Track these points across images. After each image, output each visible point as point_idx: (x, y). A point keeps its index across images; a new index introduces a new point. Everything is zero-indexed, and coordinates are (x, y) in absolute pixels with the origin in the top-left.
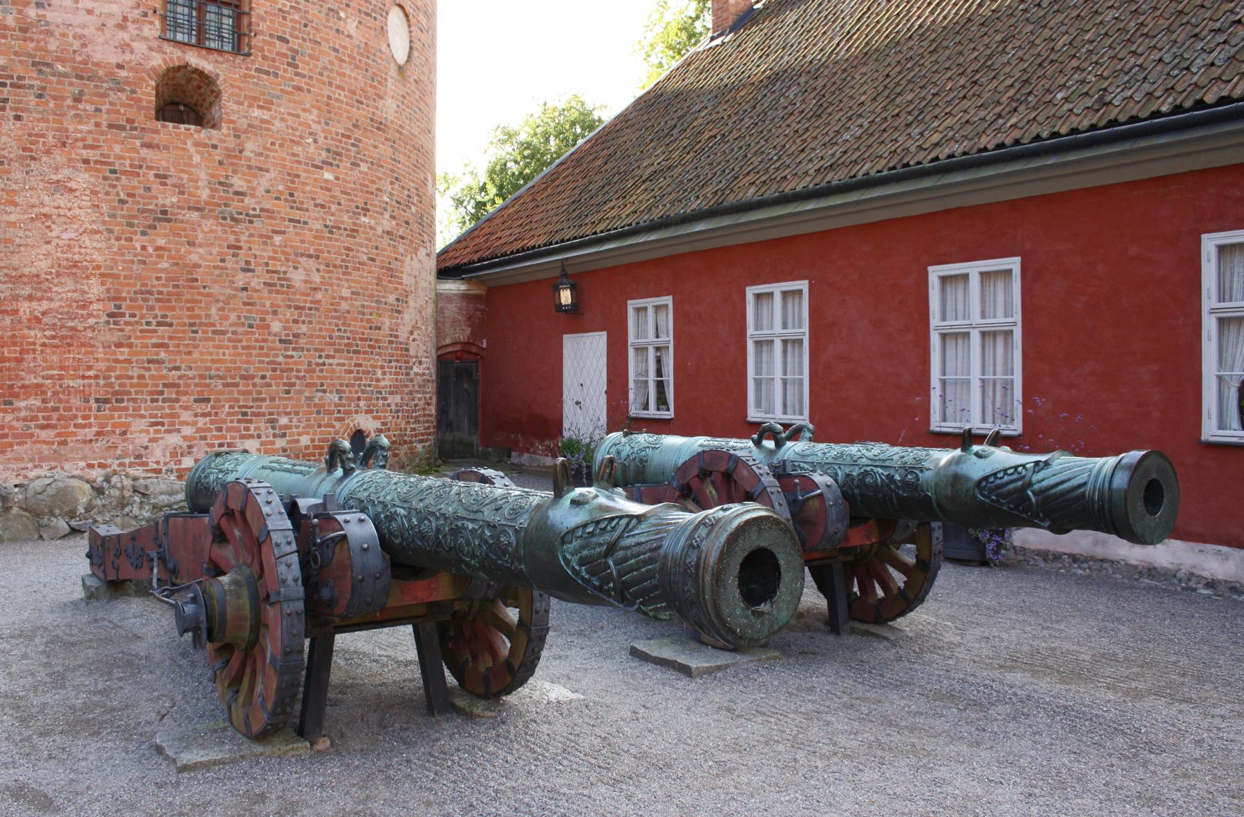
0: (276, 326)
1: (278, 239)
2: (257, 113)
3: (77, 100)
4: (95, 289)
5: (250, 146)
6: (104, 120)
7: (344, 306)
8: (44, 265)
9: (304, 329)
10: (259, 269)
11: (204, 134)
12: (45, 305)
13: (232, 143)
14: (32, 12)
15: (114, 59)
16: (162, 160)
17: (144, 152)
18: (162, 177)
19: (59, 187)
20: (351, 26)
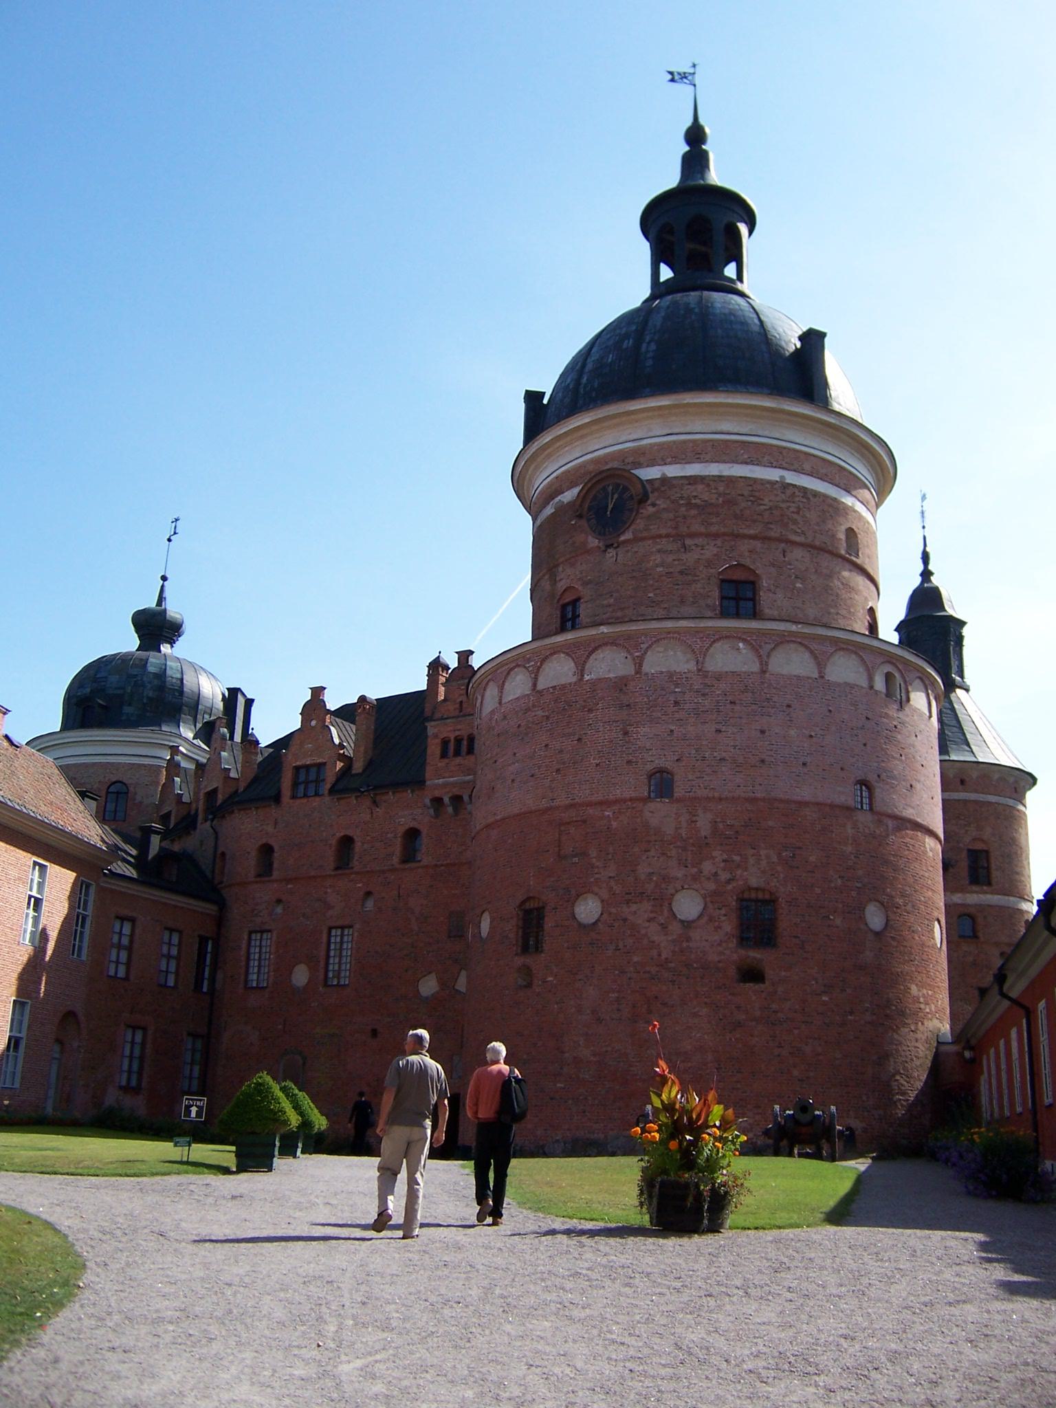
0: (796, 1073)
1: (796, 1032)
4: (710, 1057)
5: (780, 989)
9: (812, 1074)
11: (758, 987)
14: (685, 945)
15: (716, 959)
18: (738, 1008)
19: (695, 1015)
20: (838, 922)
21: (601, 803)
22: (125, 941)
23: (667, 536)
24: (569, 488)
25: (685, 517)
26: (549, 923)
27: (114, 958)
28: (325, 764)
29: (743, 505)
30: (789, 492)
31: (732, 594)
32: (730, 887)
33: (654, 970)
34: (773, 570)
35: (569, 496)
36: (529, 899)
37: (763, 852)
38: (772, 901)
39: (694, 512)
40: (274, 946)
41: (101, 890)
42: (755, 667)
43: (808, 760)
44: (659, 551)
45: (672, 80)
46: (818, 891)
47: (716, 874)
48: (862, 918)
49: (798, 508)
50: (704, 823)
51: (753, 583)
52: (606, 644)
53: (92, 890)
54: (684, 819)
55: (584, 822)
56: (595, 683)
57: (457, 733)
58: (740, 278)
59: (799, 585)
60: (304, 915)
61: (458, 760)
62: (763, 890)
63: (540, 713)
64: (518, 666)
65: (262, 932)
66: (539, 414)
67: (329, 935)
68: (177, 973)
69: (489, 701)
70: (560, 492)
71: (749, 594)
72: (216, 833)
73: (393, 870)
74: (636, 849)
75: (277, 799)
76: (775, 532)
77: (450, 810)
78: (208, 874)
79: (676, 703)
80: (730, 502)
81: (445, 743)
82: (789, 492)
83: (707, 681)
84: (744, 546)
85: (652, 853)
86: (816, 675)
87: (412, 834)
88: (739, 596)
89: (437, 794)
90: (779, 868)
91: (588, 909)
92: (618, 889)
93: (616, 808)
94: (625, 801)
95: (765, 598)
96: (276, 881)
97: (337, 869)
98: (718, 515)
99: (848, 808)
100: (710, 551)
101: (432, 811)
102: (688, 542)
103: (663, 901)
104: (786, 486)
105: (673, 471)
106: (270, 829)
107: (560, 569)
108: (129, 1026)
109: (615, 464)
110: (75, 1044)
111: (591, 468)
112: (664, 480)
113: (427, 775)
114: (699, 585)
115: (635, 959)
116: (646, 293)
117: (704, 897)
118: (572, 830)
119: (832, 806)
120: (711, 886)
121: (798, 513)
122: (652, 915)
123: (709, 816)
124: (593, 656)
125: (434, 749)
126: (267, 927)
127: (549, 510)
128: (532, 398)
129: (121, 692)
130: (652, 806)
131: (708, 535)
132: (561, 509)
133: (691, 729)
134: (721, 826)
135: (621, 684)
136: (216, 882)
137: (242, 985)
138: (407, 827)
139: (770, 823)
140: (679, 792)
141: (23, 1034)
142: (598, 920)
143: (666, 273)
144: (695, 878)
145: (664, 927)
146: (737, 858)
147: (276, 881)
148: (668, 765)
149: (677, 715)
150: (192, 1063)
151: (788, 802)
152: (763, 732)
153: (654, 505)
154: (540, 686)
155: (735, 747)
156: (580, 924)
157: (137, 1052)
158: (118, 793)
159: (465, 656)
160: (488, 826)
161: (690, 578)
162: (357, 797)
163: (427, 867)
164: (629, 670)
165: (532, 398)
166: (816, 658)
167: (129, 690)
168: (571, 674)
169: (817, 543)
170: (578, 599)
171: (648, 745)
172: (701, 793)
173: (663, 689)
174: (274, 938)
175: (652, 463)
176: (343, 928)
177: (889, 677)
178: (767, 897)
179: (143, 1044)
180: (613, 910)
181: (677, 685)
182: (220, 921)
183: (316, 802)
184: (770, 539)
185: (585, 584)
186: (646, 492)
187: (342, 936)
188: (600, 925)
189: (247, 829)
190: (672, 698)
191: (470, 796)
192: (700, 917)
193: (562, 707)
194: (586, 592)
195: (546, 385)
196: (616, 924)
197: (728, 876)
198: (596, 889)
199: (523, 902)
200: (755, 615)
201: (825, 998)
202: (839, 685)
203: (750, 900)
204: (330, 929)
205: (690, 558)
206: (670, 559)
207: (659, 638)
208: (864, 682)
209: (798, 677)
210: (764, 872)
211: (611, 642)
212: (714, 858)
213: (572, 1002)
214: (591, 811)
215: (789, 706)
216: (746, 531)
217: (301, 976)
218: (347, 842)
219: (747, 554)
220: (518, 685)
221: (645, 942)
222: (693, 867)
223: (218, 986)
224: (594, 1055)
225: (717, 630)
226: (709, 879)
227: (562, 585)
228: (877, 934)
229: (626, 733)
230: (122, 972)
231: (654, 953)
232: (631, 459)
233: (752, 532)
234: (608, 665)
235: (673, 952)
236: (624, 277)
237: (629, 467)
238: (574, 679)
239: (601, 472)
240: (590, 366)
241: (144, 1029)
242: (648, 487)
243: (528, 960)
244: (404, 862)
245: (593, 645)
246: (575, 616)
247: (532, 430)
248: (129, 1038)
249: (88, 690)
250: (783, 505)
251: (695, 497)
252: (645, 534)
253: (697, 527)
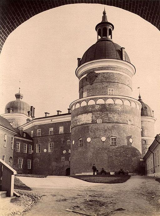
24: (85, 74)
35: (85, 75)
40: (44, 149)
58: (111, 38)
66: (81, 62)
76: (116, 81)
111: (88, 71)
116: (96, 41)
143: (100, 37)
186: (97, 76)
195: (81, 57)
205: (104, 86)
220: (78, 106)
236: (93, 38)
247: (79, 65)
253: (105, 81)
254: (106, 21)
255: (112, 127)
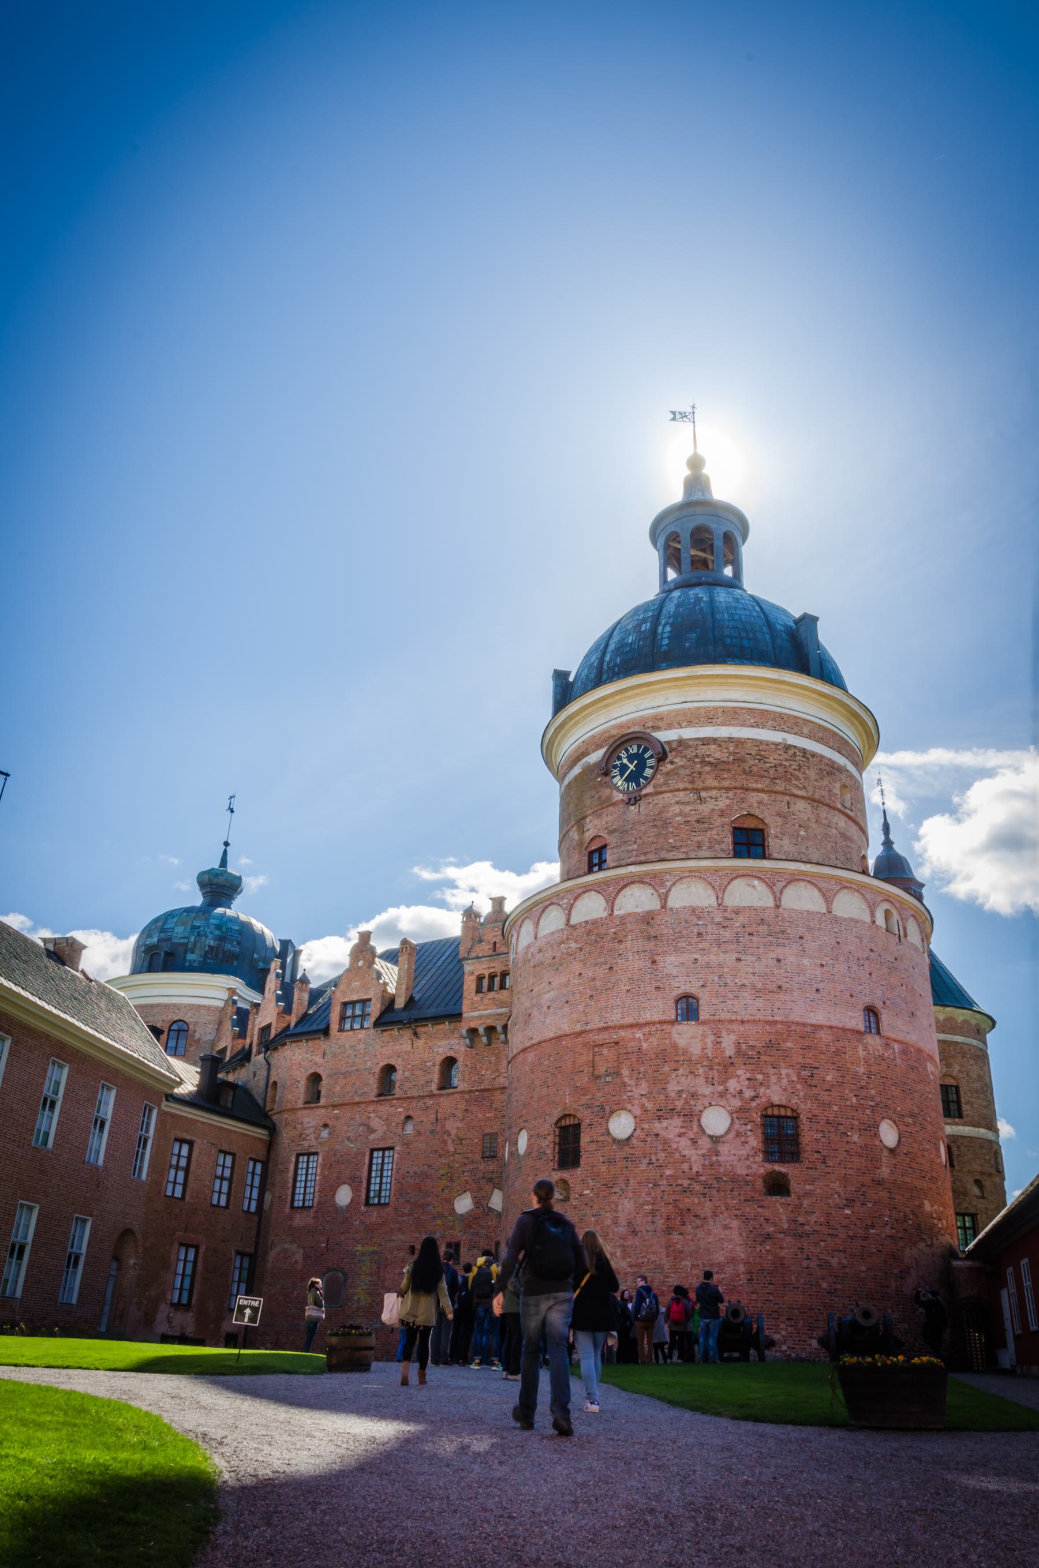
0: (824, 1285)
1: (822, 1244)
2: (808, 1187)
3: (732, 1191)
4: (742, 1268)
5: (806, 1202)
6: (742, 1198)
7: (863, 1275)
8: (722, 1259)
9: (839, 1286)
10: (814, 1259)
11: (784, 1200)
12: (723, 1276)
13: (797, 1202)
14: (714, 1158)
15: (745, 1172)
16: (766, 1213)
17: (759, 1210)
19: (726, 1227)
20: (855, 1138)
21: (631, 1026)
22: (183, 1163)
23: (685, 789)
25: (700, 773)
26: (585, 1139)
27: (171, 1178)
28: (370, 1000)
29: (751, 762)
30: (791, 752)
31: (744, 840)
32: (754, 1104)
33: (686, 1183)
34: (779, 820)
35: (596, 757)
36: (565, 1116)
37: (784, 1072)
38: (795, 1118)
39: (708, 768)
41: (162, 1114)
42: (770, 903)
43: (821, 986)
44: (677, 803)
45: (674, 419)
46: (835, 1108)
47: (741, 1092)
48: (876, 1135)
49: (799, 765)
50: (728, 1044)
51: (762, 831)
52: (633, 882)
53: (155, 1113)
54: (710, 1039)
55: (617, 1043)
56: (623, 918)
57: (492, 970)
59: (802, 833)
60: (348, 1138)
61: (492, 995)
62: (785, 1107)
63: (573, 945)
64: (552, 904)
65: (309, 1154)
66: (565, 691)
67: (371, 1158)
68: (229, 1194)
69: (524, 938)
70: (585, 754)
71: (759, 841)
72: (269, 1064)
73: (431, 1096)
74: (666, 1068)
75: (326, 1032)
76: (780, 786)
77: (484, 1039)
78: (260, 1102)
79: (699, 934)
80: (740, 760)
81: (480, 979)
82: (791, 752)
83: (727, 915)
84: (753, 798)
85: (681, 1071)
86: (824, 910)
87: (450, 1062)
88: (749, 841)
89: (473, 1025)
90: (799, 1087)
91: (621, 1125)
92: (649, 1106)
93: (646, 1030)
94: (654, 1023)
95: (772, 843)
96: (324, 1107)
97: (379, 1095)
98: (729, 771)
99: (858, 1032)
100: (723, 803)
101: (467, 1041)
102: (703, 794)
103: (691, 1117)
104: (787, 747)
105: (688, 733)
106: (318, 1059)
107: (588, 820)
108: (181, 1244)
109: (637, 729)
110: (132, 1262)
111: (614, 732)
112: (681, 742)
113: (464, 1009)
114: (714, 832)
115: (668, 1172)
117: (731, 1114)
118: (605, 1051)
119: (844, 1030)
120: (737, 1103)
121: (799, 770)
122: (683, 1130)
123: (733, 1037)
124: (623, 893)
125: (469, 984)
126: (313, 1150)
127: (577, 770)
128: (560, 676)
129: (186, 941)
130: (678, 1028)
131: (719, 789)
132: (588, 770)
133: (712, 957)
134: (744, 1046)
135: (648, 918)
136: (268, 1109)
137: (288, 1205)
138: (444, 1056)
139: (789, 1045)
140: (704, 1015)
141: (84, 1249)
142: (632, 1135)
143: (672, 575)
144: (722, 1095)
145: (694, 1142)
146: (760, 1077)
147: (324, 1107)
148: (693, 990)
149: (700, 946)
150: (239, 1282)
151: (804, 1025)
152: (779, 960)
153: (672, 763)
154: (573, 922)
155: (754, 974)
156: (614, 1140)
157: (189, 1271)
158: (179, 1031)
159: (498, 902)
160: (524, 1050)
161: (706, 825)
162: (399, 1029)
163: (462, 1092)
164: (655, 904)
165: (560, 676)
166: (824, 895)
167: (192, 939)
168: (601, 909)
169: (817, 796)
170: (605, 846)
171: (674, 972)
172: (723, 1016)
173: (687, 922)
174: (320, 1160)
175: (670, 726)
176: (384, 1150)
177: (887, 914)
178: (789, 1114)
179: (195, 1262)
180: (646, 1126)
181: (699, 918)
182: (271, 1145)
183: (362, 1034)
184: (775, 792)
185: (611, 832)
187: (383, 1157)
188: (634, 1141)
189: (295, 1061)
190: (695, 930)
191: (505, 1027)
192: (728, 1132)
193: (596, 939)
194: (612, 840)
195: (573, 667)
196: (649, 1139)
197: (753, 1094)
198: (629, 1106)
199: (559, 1120)
200: (764, 856)
201: (847, 1212)
202: (845, 920)
203: (773, 1116)
204: (372, 1151)
206: (687, 809)
207: (681, 877)
208: (867, 919)
209: (808, 912)
210: (785, 1090)
211: (639, 880)
212: (738, 1076)
213: (608, 1214)
214: (622, 1033)
215: (801, 938)
216: (754, 786)
217: (344, 1196)
218: (390, 1069)
219: (755, 805)
220: (553, 921)
221: (677, 1155)
222: (719, 1084)
223: (266, 1207)
224: (631, 1266)
225: (734, 869)
226: (735, 1096)
227: (589, 835)
228: (892, 1151)
229: (654, 962)
230: (178, 1193)
231: (686, 1166)
232: (650, 724)
233: (760, 786)
234: (637, 900)
235: (704, 1165)
237: (648, 731)
238: (605, 914)
239: (623, 736)
240: (612, 646)
241: (197, 1248)
242: (667, 748)
243: (565, 1175)
244: (441, 1088)
245: (622, 883)
246: (602, 862)
247: (560, 705)
248: (182, 1256)
249: (155, 940)
250: (787, 763)
251: (708, 756)
252: (665, 788)
253: (710, 782)
254: (708, 497)
255: (769, 1045)
